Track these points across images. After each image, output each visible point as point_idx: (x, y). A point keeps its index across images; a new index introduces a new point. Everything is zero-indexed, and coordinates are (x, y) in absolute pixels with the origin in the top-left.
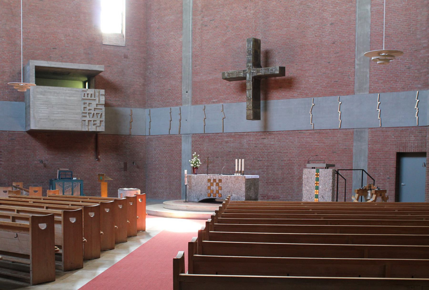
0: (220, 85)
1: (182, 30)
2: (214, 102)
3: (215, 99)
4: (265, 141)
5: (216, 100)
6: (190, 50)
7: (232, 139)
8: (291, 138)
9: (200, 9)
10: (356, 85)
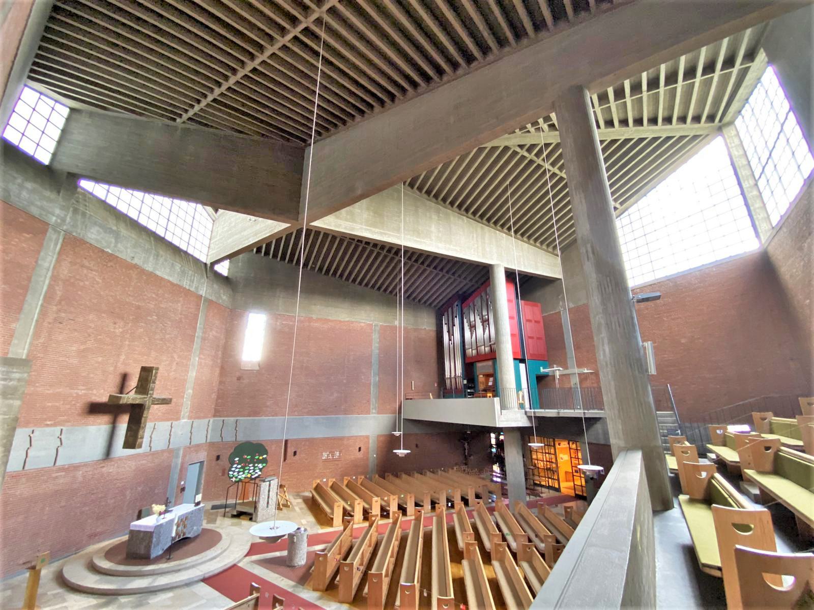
1: (19, 313)
3: (50, 421)
4: (104, 469)
6: (27, 347)
7: (63, 473)
8: (129, 462)
9: (58, 298)
10: (182, 413)
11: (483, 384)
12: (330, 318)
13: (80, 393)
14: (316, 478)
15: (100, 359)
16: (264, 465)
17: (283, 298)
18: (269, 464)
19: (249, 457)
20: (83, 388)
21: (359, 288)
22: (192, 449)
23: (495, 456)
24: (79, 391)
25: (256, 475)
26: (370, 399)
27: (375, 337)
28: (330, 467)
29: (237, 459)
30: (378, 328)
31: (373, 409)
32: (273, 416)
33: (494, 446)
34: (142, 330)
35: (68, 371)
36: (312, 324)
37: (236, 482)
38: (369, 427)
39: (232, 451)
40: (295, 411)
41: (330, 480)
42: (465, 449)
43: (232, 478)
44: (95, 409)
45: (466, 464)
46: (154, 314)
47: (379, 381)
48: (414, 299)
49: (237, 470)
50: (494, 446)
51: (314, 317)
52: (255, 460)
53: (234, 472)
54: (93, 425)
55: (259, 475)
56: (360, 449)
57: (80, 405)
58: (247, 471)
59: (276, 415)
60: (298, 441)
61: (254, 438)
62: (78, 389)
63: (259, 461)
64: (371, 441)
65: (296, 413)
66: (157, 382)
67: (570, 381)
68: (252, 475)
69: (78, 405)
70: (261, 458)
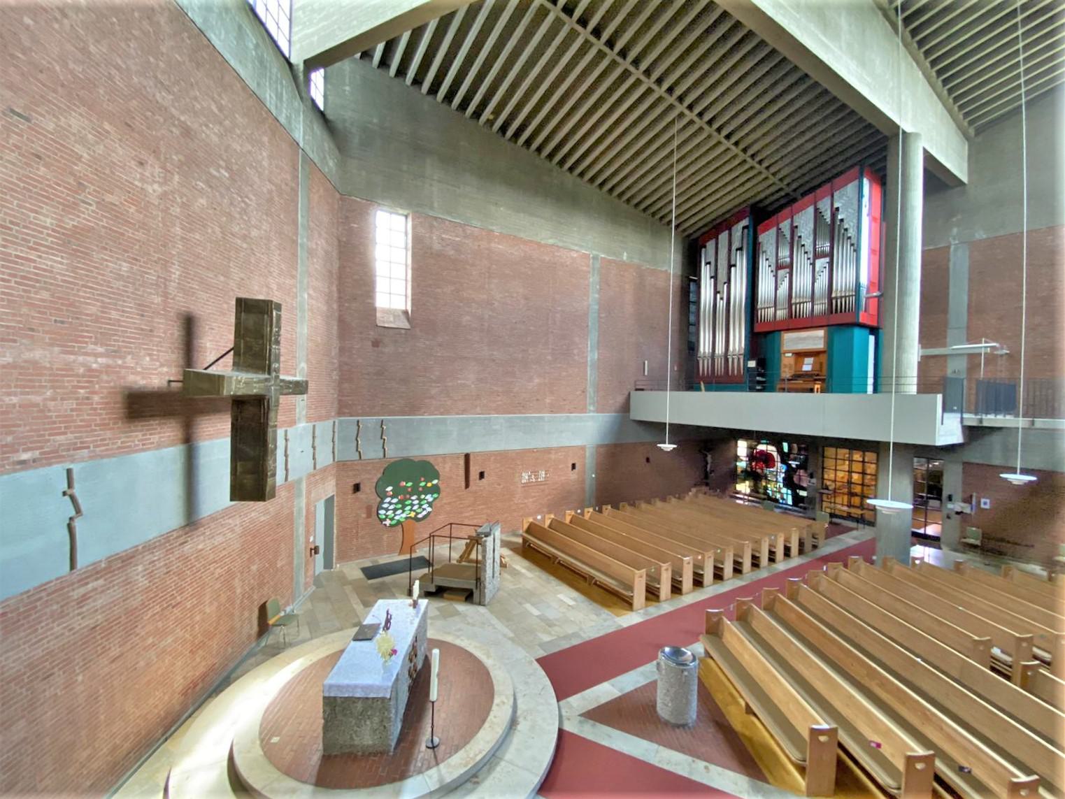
0: (49, 393)
2: (23, 462)
3: (25, 450)
4: (187, 547)
5: (37, 453)
7: (101, 582)
8: (230, 521)
10: (297, 410)
11: (790, 369)
12: (522, 235)
13: (94, 366)
14: (529, 515)
15: (125, 267)
16: (435, 495)
17: (439, 182)
18: (443, 494)
19: (410, 484)
20: (100, 350)
21: (570, 180)
22: (317, 477)
23: (742, 472)
24: (91, 359)
25: (424, 513)
26: (585, 388)
27: (593, 279)
28: (533, 494)
29: (389, 489)
30: (598, 265)
31: (590, 404)
32: (442, 414)
33: (744, 459)
34: (203, 201)
35: (45, 295)
36: (493, 245)
37: (391, 526)
38: (581, 431)
39: (379, 475)
40: (476, 406)
41: (547, 516)
42: (707, 463)
43: (385, 520)
44: (140, 406)
45: (707, 484)
46: (222, 163)
47: (598, 359)
48: (654, 214)
49: (392, 507)
50: (744, 459)
51: (497, 230)
52: (420, 489)
53: (387, 510)
54: (143, 450)
55: (429, 513)
56: (574, 466)
57: (101, 398)
58: (409, 508)
59: (447, 412)
60: (488, 456)
61: (415, 453)
62: (86, 354)
63: (427, 491)
64: (588, 454)
65: (478, 409)
66: (282, 339)
67: (946, 367)
68: (417, 514)
69: (96, 398)
70: (429, 485)
